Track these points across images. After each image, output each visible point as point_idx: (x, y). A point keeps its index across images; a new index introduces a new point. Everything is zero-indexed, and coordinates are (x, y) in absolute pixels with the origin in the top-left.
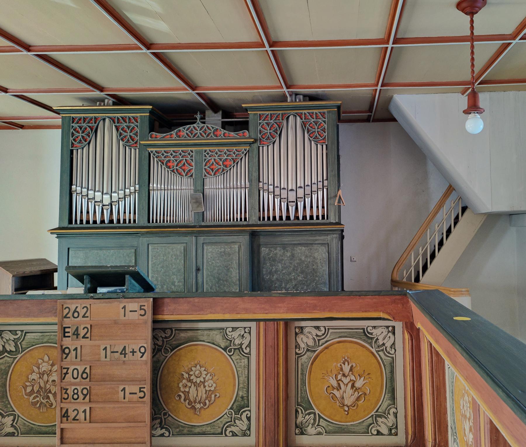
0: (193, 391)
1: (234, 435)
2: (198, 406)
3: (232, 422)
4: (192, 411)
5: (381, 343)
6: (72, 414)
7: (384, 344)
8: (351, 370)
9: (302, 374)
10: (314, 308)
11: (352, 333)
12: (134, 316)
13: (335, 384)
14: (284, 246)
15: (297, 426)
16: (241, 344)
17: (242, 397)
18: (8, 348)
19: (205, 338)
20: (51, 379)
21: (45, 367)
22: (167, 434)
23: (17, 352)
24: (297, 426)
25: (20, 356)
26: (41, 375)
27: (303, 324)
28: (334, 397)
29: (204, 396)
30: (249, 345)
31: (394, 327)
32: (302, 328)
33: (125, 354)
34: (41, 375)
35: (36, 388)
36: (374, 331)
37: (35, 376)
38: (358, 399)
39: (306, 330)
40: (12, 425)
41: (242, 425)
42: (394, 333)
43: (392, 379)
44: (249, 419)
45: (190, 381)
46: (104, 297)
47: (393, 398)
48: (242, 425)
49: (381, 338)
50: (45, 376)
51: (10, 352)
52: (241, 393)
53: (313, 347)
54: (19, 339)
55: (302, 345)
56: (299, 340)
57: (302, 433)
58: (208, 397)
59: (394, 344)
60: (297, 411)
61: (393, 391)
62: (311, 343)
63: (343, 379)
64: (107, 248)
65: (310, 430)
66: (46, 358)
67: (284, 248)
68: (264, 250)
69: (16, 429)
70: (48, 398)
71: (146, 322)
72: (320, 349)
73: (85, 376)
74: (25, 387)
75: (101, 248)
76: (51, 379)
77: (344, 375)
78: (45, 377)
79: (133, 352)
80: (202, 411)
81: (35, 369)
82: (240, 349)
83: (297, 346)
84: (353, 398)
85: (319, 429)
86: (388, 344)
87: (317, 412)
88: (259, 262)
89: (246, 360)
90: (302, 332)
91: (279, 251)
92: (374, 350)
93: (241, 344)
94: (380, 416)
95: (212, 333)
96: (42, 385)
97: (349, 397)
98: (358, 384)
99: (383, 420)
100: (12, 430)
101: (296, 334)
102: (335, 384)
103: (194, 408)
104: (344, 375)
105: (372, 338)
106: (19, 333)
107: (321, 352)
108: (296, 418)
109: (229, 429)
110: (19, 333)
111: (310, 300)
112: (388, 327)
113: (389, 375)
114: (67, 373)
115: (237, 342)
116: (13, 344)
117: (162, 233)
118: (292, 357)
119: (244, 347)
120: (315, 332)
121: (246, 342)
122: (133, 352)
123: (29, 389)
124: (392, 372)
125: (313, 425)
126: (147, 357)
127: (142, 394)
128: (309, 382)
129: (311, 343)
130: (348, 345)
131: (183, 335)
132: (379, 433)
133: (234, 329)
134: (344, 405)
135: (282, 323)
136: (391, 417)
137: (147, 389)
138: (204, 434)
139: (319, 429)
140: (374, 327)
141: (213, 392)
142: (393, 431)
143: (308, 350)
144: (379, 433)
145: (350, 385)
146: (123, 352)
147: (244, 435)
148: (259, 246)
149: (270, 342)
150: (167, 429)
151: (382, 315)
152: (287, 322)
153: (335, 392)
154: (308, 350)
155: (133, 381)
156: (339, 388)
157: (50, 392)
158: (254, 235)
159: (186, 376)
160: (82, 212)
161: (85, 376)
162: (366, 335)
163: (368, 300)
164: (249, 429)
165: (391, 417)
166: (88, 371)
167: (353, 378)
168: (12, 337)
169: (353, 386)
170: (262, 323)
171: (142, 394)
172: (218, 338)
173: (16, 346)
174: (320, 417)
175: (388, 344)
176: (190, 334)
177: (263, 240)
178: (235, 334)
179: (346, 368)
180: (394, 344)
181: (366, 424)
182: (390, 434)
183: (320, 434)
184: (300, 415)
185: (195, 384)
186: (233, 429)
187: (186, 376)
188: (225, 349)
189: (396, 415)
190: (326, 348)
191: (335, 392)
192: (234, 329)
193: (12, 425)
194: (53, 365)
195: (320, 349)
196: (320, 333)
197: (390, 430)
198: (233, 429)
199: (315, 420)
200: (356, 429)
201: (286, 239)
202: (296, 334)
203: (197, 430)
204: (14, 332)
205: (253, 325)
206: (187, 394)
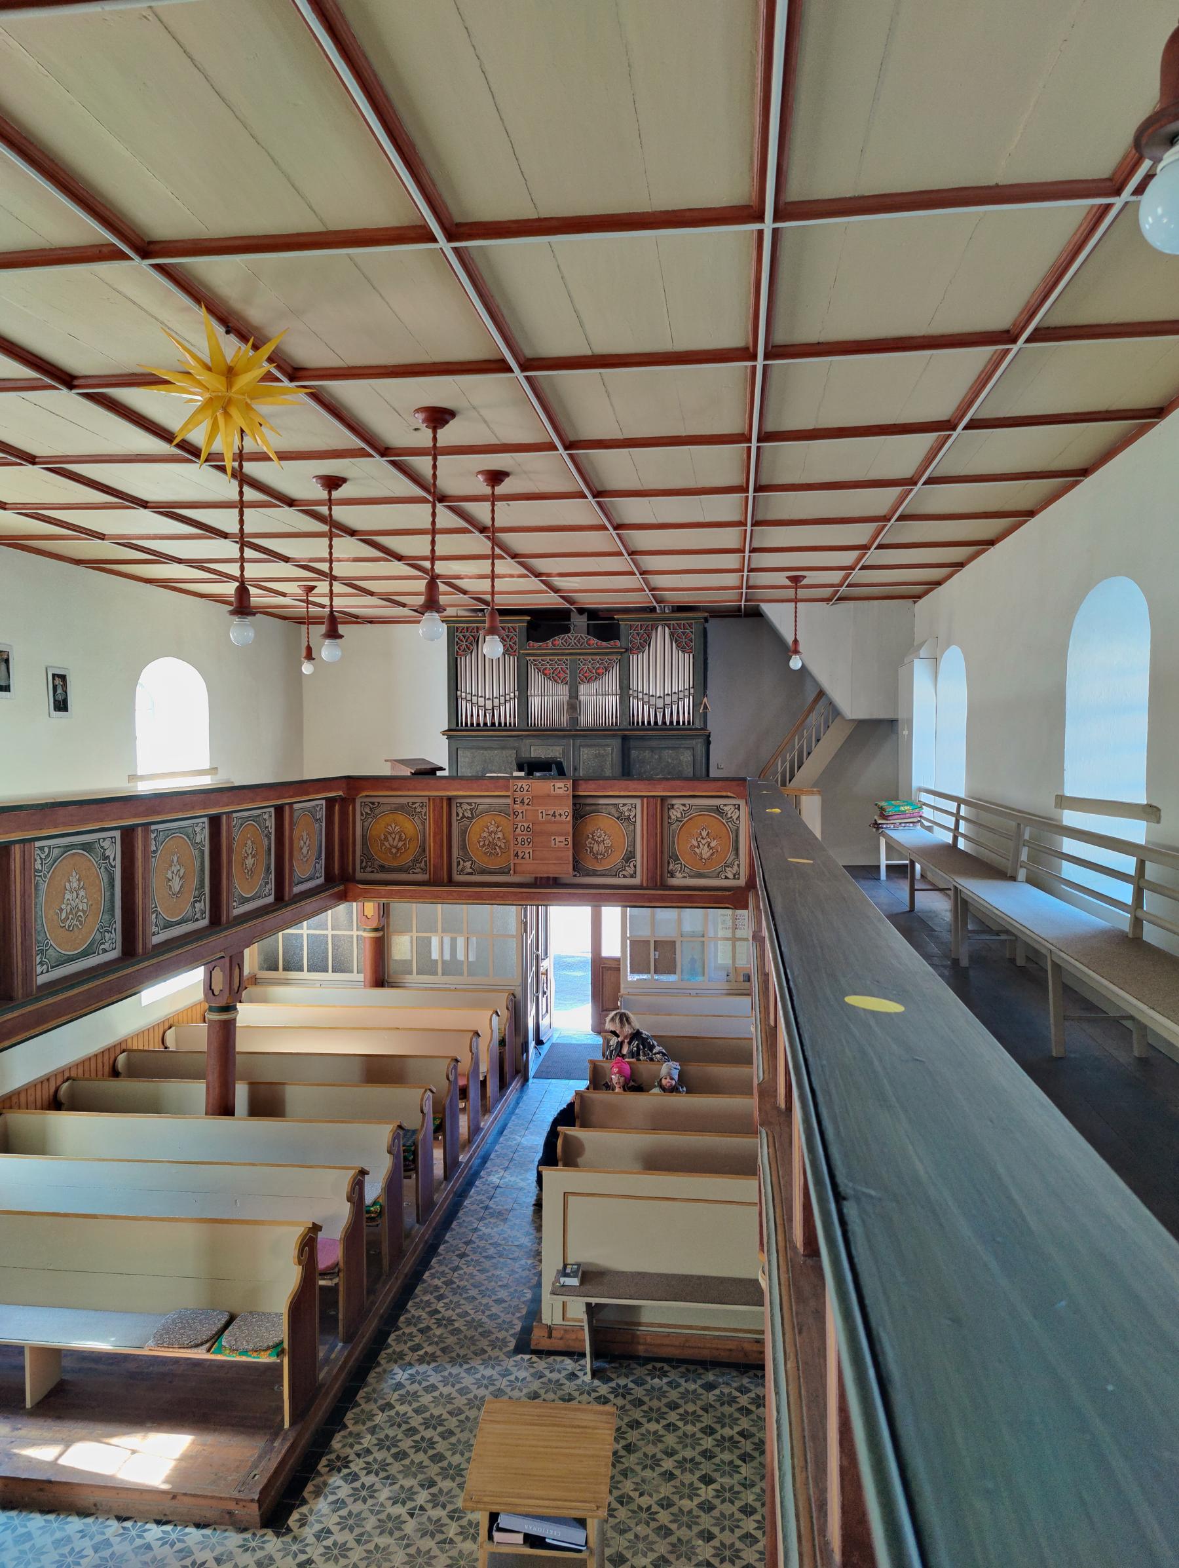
0: (596, 847)
1: (625, 876)
2: (599, 857)
3: (623, 869)
4: (596, 860)
5: (729, 816)
6: (521, 855)
7: (731, 817)
8: (708, 834)
9: (673, 837)
10: (682, 789)
11: (709, 809)
12: (561, 792)
13: (696, 844)
14: (652, 749)
15: (669, 872)
16: (630, 815)
17: (630, 852)
18: (466, 815)
19: (604, 811)
20: (497, 836)
21: (492, 828)
22: (578, 875)
23: (473, 817)
24: (669, 872)
25: (474, 820)
26: (490, 833)
27: (674, 801)
28: (695, 853)
29: (604, 850)
30: (635, 816)
31: (739, 806)
32: (673, 805)
33: (555, 816)
34: (490, 833)
35: (487, 843)
36: (725, 808)
37: (485, 834)
38: (712, 855)
39: (676, 807)
40: (471, 868)
41: (630, 870)
42: (739, 810)
43: (737, 841)
44: (635, 866)
45: (594, 840)
46: (539, 778)
47: (737, 854)
48: (630, 870)
49: (729, 813)
50: (493, 834)
51: (468, 818)
52: (629, 849)
53: (680, 818)
54: (473, 808)
55: (673, 817)
56: (671, 813)
57: (672, 877)
58: (607, 851)
59: (739, 817)
60: (669, 862)
61: (737, 850)
62: (679, 815)
63: (702, 841)
64: (491, 749)
65: (678, 875)
66: (493, 823)
67: (652, 751)
68: (634, 753)
69: (473, 870)
70: (495, 849)
71: (568, 795)
72: (686, 819)
73: (529, 830)
74: (479, 842)
75: (485, 749)
76: (497, 836)
77: (702, 838)
78: (493, 834)
79: (560, 815)
80: (603, 861)
81: (486, 829)
82: (629, 818)
83: (669, 818)
84: (709, 854)
85: (684, 874)
86: (735, 817)
87: (683, 863)
88: (629, 763)
89: (633, 827)
90: (673, 808)
91: (647, 754)
92: (724, 821)
93: (630, 815)
94: (728, 866)
95: (608, 807)
96: (491, 840)
97: (706, 853)
98: (713, 845)
99: (730, 869)
100: (470, 871)
101: (669, 809)
102: (696, 844)
103: (596, 858)
104: (702, 838)
105: (723, 813)
106: (474, 805)
107: (686, 822)
108: (668, 866)
109: (621, 873)
110: (474, 805)
111: (678, 783)
112: (735, 805)
113: (735, 839)
114: (516, 828)
115: (627, 814)
116: (469, 812)
117: (543, 735)
118: (666, 825)
119: (631, 817)
120: (682, 808)
121: (632, 814)
122: (560, 815)
123: (482, 843)
124: (737, 836)
125: (680, 871)
126: (570, 818)
127: (567, 843)
128: (678, 843)
129: (679, 815)
130: (706, 817)
131: (588, 808)
132: (726, 878)
133: (624, 805)
134: (702, 858)
135: (659, 799)
136: (736, 867)
137: (570, 839)
138: (603, 875)
139: (684, 874)
140: (725, 805)
141: (610, 848)
142: (736, 876)
143: (677, 820)
144: (726, 878)
145: (706, 845)
146: (554, 815)
147: (632, 876)
148: (629, 748)
149: (651, 813)
150: (578, 872)
151: (729, 794)
152: (663, 798)
153: (696, 850)
154: (677, 820)
155: (560, 835)
156: (699, 847)
157: (497, 845)
158: (625, 738)
159: (591, 836)
160: (472, 716)
161: (529, 830)
162: (718, 810)
163: (720, 784)
164: (635, 873)
165: (736, 867)
166: (530, 826)
167: (709, 840)
168: (469, 807)
169: (709, 846)
170: (645, 799)
171: (567, 843)
172: (613, 811)
173: (472, 814)
174: (685, 866)
175: (735, 817)
176: (594, 807)
177: (632, 743)
178: (625, 809)
179: (704, 833)
180: (739, 817)
181: (717, 871)
182: (734, 878)
183: (685, 877)
184: (671, 865)
185: (597, 842)
186: (624, 873)
187: (591, 836)
188: (618, 819)
189: (739, 866)
190: (690, 819)
191: (696, 850)
192: (624, 805)
193: (471, 868)
194: (498, 827)
195: (686, 819)
196: (685, 809)
197: (734, 876)
198: (624, 873)
199: (681, 868)
200: (711, 875)
201: (654, 743)
202: (669, 809)
203: (599, 873)
204: (470, 804)
205: (638, 802)
206: (591, 848)
